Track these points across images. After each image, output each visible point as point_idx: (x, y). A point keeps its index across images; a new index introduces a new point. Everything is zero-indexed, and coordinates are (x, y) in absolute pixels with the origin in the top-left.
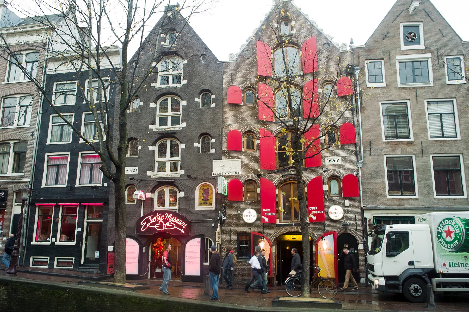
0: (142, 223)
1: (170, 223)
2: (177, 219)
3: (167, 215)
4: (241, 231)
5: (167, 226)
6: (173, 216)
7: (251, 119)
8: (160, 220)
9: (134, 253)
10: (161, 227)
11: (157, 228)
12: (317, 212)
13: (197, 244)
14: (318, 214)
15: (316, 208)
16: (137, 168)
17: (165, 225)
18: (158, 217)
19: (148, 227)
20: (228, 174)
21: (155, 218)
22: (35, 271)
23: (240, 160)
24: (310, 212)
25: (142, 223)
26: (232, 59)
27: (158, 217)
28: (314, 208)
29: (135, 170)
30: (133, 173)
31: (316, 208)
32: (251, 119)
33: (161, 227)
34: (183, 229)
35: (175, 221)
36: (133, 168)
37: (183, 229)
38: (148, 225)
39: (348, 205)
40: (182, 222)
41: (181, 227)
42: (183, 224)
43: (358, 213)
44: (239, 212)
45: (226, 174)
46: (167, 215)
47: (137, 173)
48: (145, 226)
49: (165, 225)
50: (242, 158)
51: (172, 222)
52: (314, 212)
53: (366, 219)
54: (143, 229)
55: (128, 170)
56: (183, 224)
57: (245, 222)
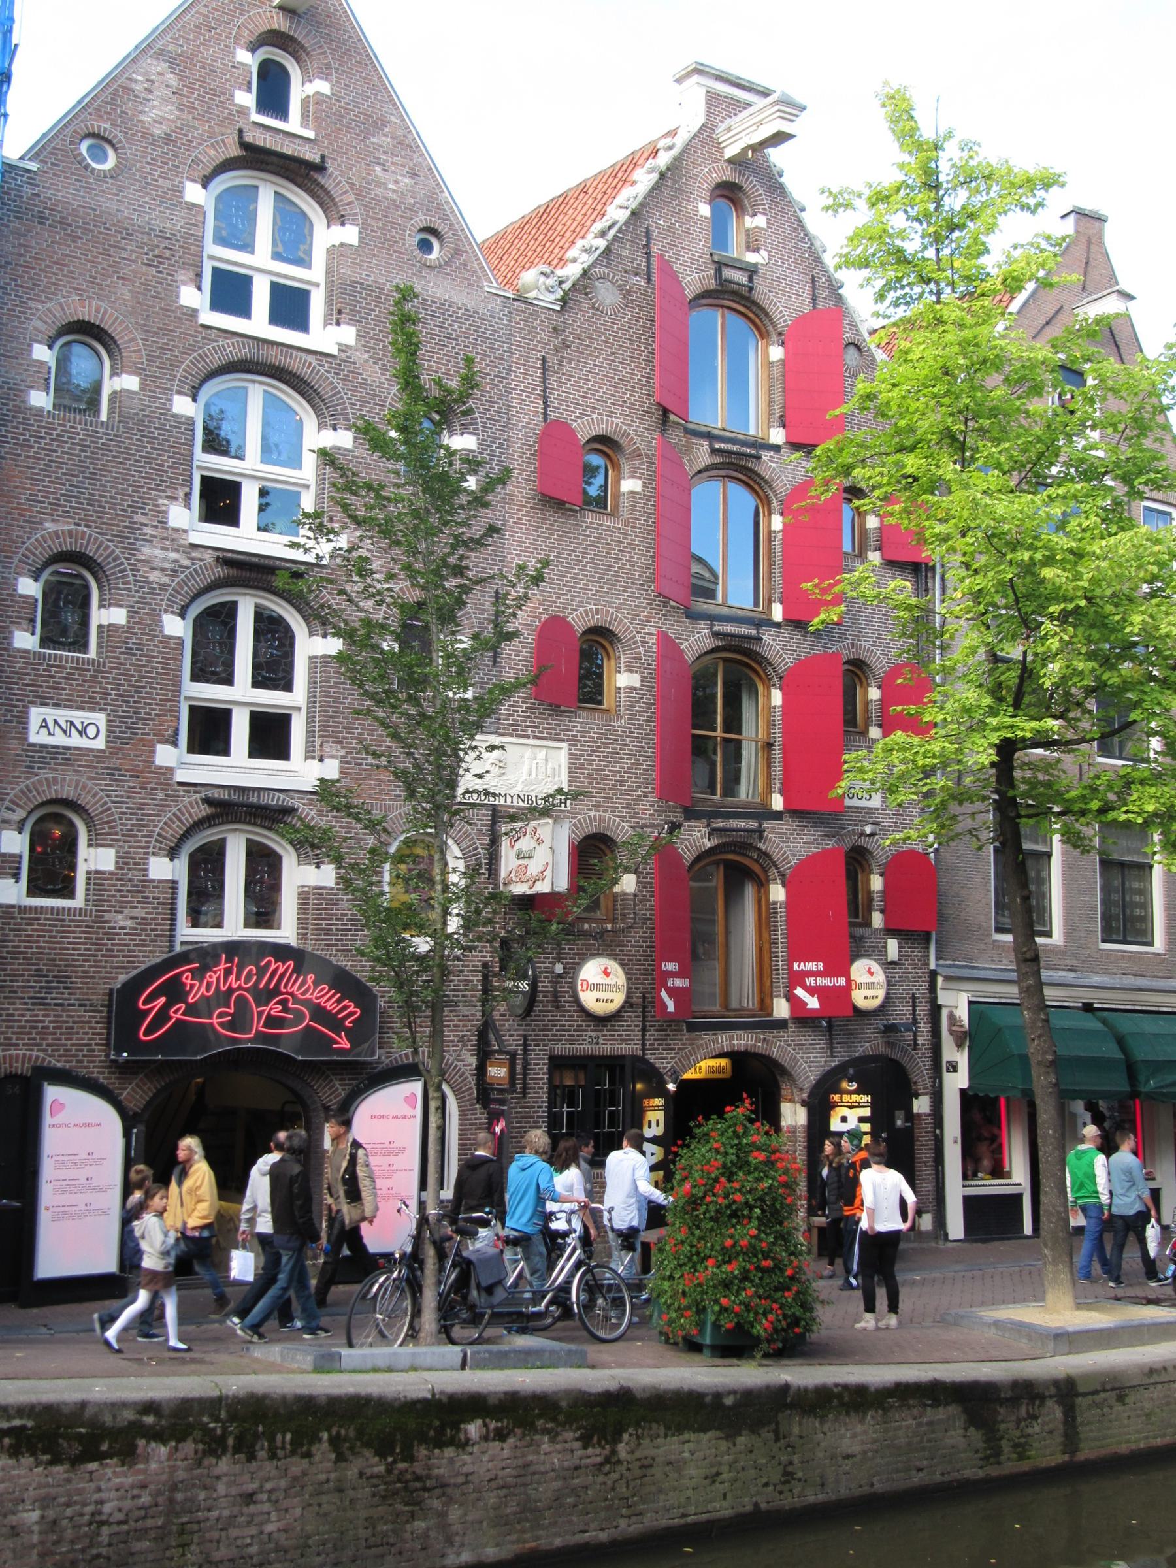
0: (145, 1003)
1: (283, 1003)
2: (316, 984)
3: (269, 963)
4: (563, 1048)
5: (269, 1015)
6: (298, 970)
7: (610, 583)
8: (235, 986)
9: (98, 1162)
10: (238, 1022)
11: (221, 1024)
12: (822, 981)
13: (406, 1110)
14: (826, 988)
15: (821, 966)
16: (101, 719)
17: (260, 1014)
18: (228, 972)
19: (178, 1019)
20: (521, 804)
21: (212, 977)
22: (573, 1347)
23: (565, 745)
24: (797, 979)
25: (145, 1003)
26: (547, 294)
27: (228, 972)
28: (810, 966)
29: (91, 731)
30: (75, 741)
31: (821, 966)
32: (610, 583)
33: (238, 1022)
34: (347, 1030)
35: (308, 996)
36: (79, 717)
37: (347, 1030)
38: (177, 1013)
39: (896, 959)
40: (339, 1001)
41: (334, 1022)
42: (346, 1007)
43: (922, 990)
44: (559, 969)
45: (515, 803)
46: (269, 963)
47: (100, 744)
48: (163, 1016)
49: (260, 1014)
50: (573, 741)
51: (297, 1001)
52: (810, 981)
53: (939, 1007)
54: (146, 1033)
55: (51, 724)
56: (346, 1007)
57: (582, 1009)
